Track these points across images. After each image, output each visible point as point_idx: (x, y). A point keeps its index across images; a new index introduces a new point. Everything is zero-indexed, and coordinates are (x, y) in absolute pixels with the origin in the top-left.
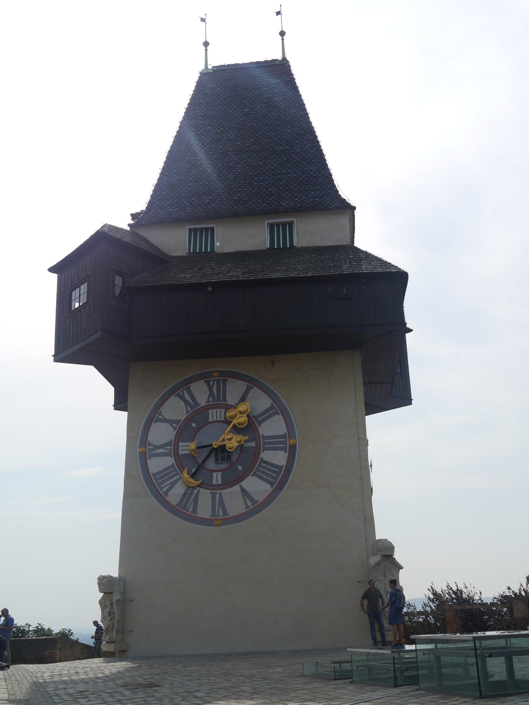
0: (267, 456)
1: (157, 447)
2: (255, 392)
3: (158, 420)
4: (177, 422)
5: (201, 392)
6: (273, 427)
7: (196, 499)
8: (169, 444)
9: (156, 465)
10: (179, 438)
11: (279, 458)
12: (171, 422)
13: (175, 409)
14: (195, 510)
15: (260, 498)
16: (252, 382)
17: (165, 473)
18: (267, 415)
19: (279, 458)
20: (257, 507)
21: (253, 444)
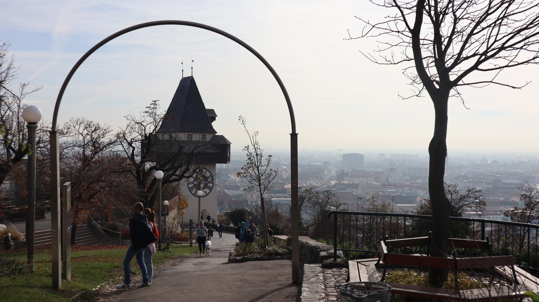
2: (208, 172)
9: (190, 186)
10: (194, 181)
11: (211, 185)
19: (211, 185)
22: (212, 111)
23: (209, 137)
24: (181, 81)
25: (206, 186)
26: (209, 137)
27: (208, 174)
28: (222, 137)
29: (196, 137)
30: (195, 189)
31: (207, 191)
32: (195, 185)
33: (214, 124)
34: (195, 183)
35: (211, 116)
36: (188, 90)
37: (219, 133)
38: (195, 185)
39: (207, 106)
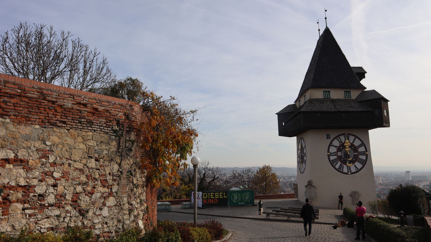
0: (361, 157)
1: (332, 153)
2: (357, 139)
3: (332, 146)
4: (337, 147)
5: (342, 138)
6: (362, 149)
7: (343, 167)
8: (335, 152)
9: (332, 158)
12: (335, 146)
13: (336, 143)
14: (343, 170)
15: (359, 168)
16: (356, 137)
17: (334, 161)
18: (360, 146)
20: (358, 171)
21: (357, 153)
22: (361, 68)
23: (354, 94)
24: (318, 41)
25: (356, 159)
26: (354, 94)
27: (357, 143)
28: (374, 92)
29: (337, 94)
30: (339, 163)
31: (359, 165)
32: (339, 158)
33: (363, 82)
34: (339, 154)
35: (361, 73)
36: (328, 49)
37: (369, 88)
38: (339, 158)
39: (353, 63)
